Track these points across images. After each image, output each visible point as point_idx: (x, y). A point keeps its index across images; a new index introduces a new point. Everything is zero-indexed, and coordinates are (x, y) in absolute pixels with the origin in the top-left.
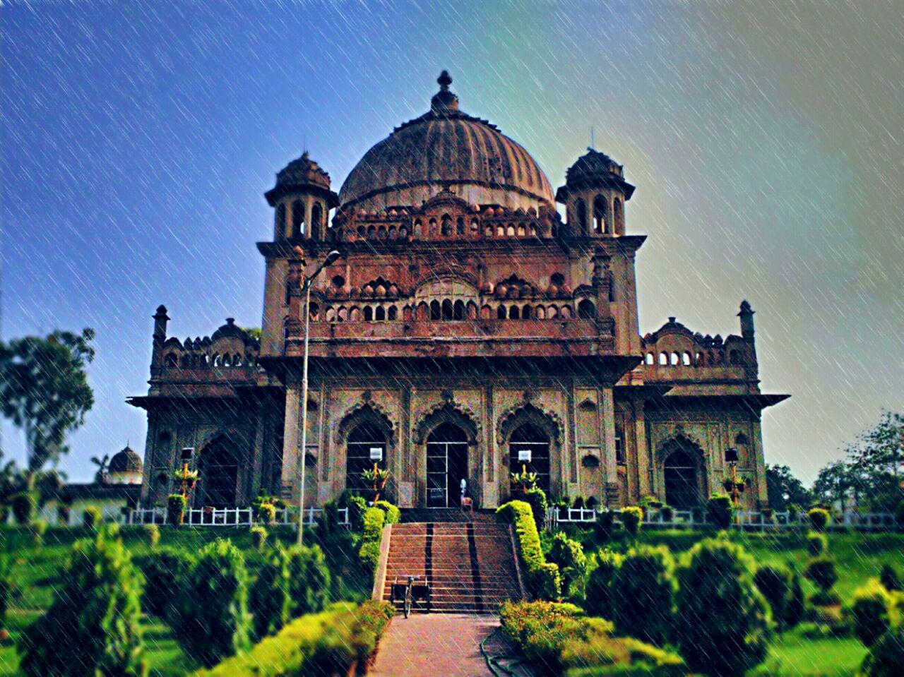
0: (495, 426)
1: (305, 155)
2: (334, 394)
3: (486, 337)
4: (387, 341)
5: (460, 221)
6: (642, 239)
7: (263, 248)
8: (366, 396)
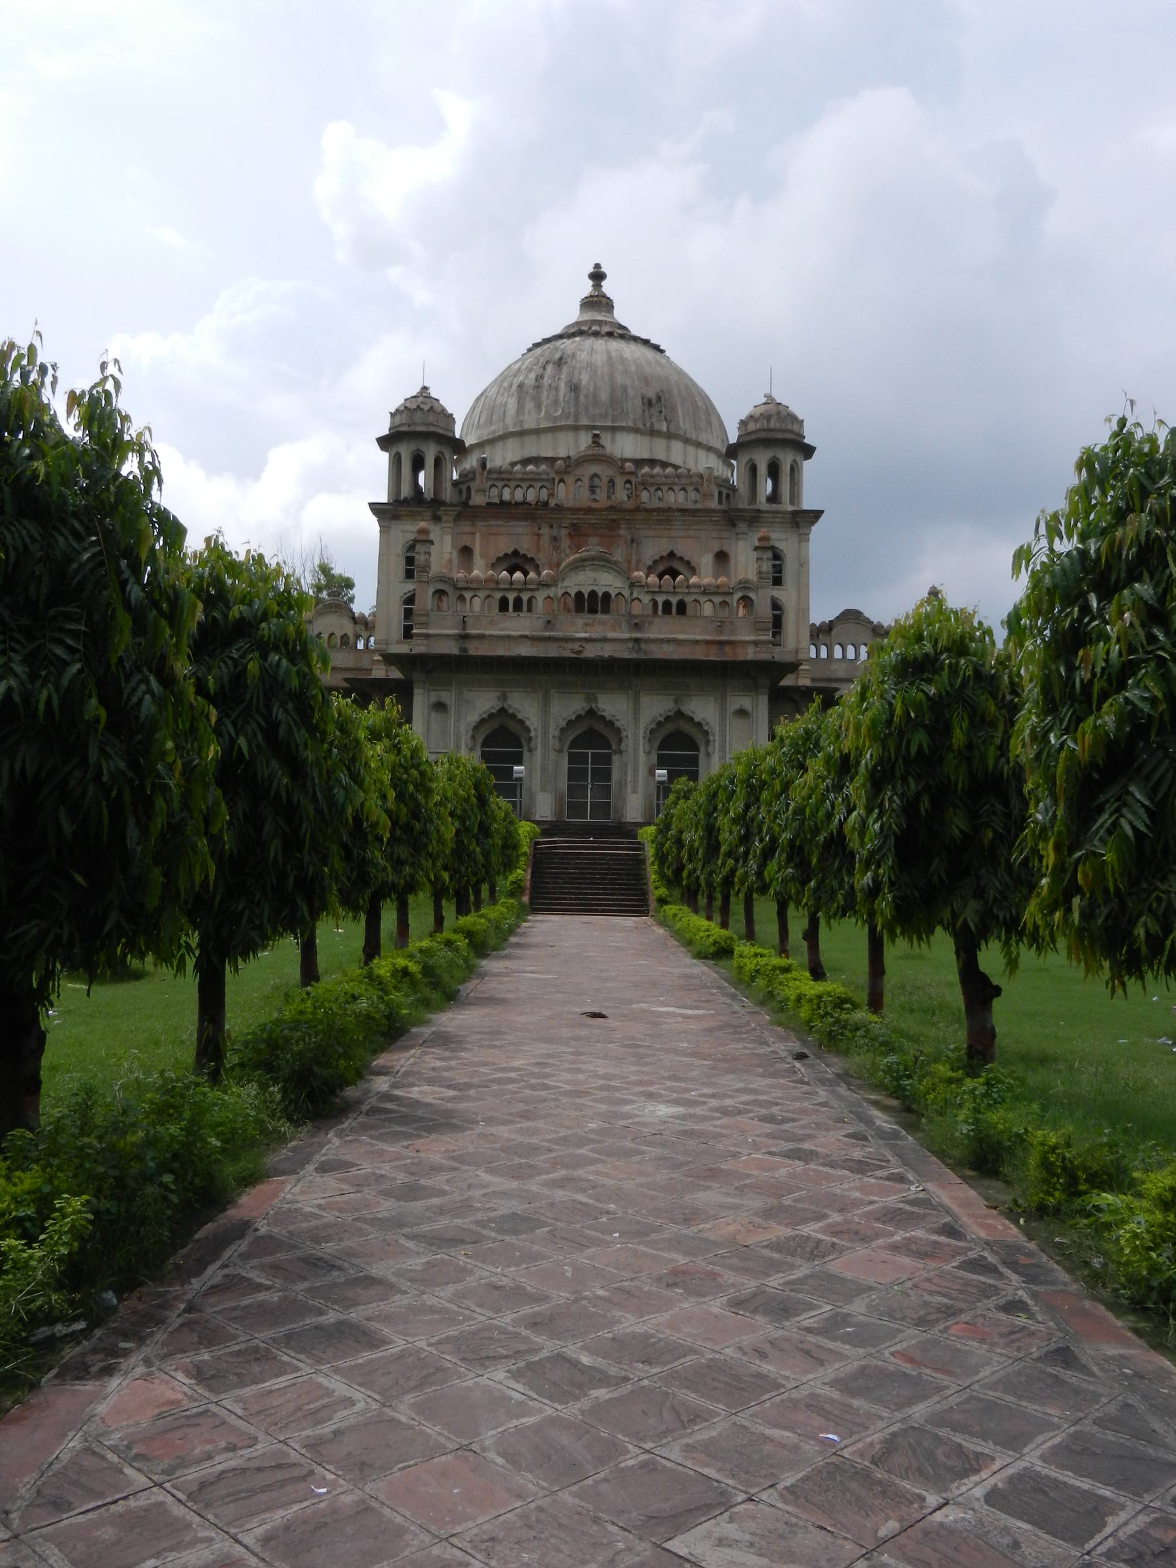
1: (425, 388)
2: (467, 695)
3: (635, 635)
4: (526, 637)
5: (612, 482)
6: (817, 514)
7: (376, 508)
8: (504, 697)
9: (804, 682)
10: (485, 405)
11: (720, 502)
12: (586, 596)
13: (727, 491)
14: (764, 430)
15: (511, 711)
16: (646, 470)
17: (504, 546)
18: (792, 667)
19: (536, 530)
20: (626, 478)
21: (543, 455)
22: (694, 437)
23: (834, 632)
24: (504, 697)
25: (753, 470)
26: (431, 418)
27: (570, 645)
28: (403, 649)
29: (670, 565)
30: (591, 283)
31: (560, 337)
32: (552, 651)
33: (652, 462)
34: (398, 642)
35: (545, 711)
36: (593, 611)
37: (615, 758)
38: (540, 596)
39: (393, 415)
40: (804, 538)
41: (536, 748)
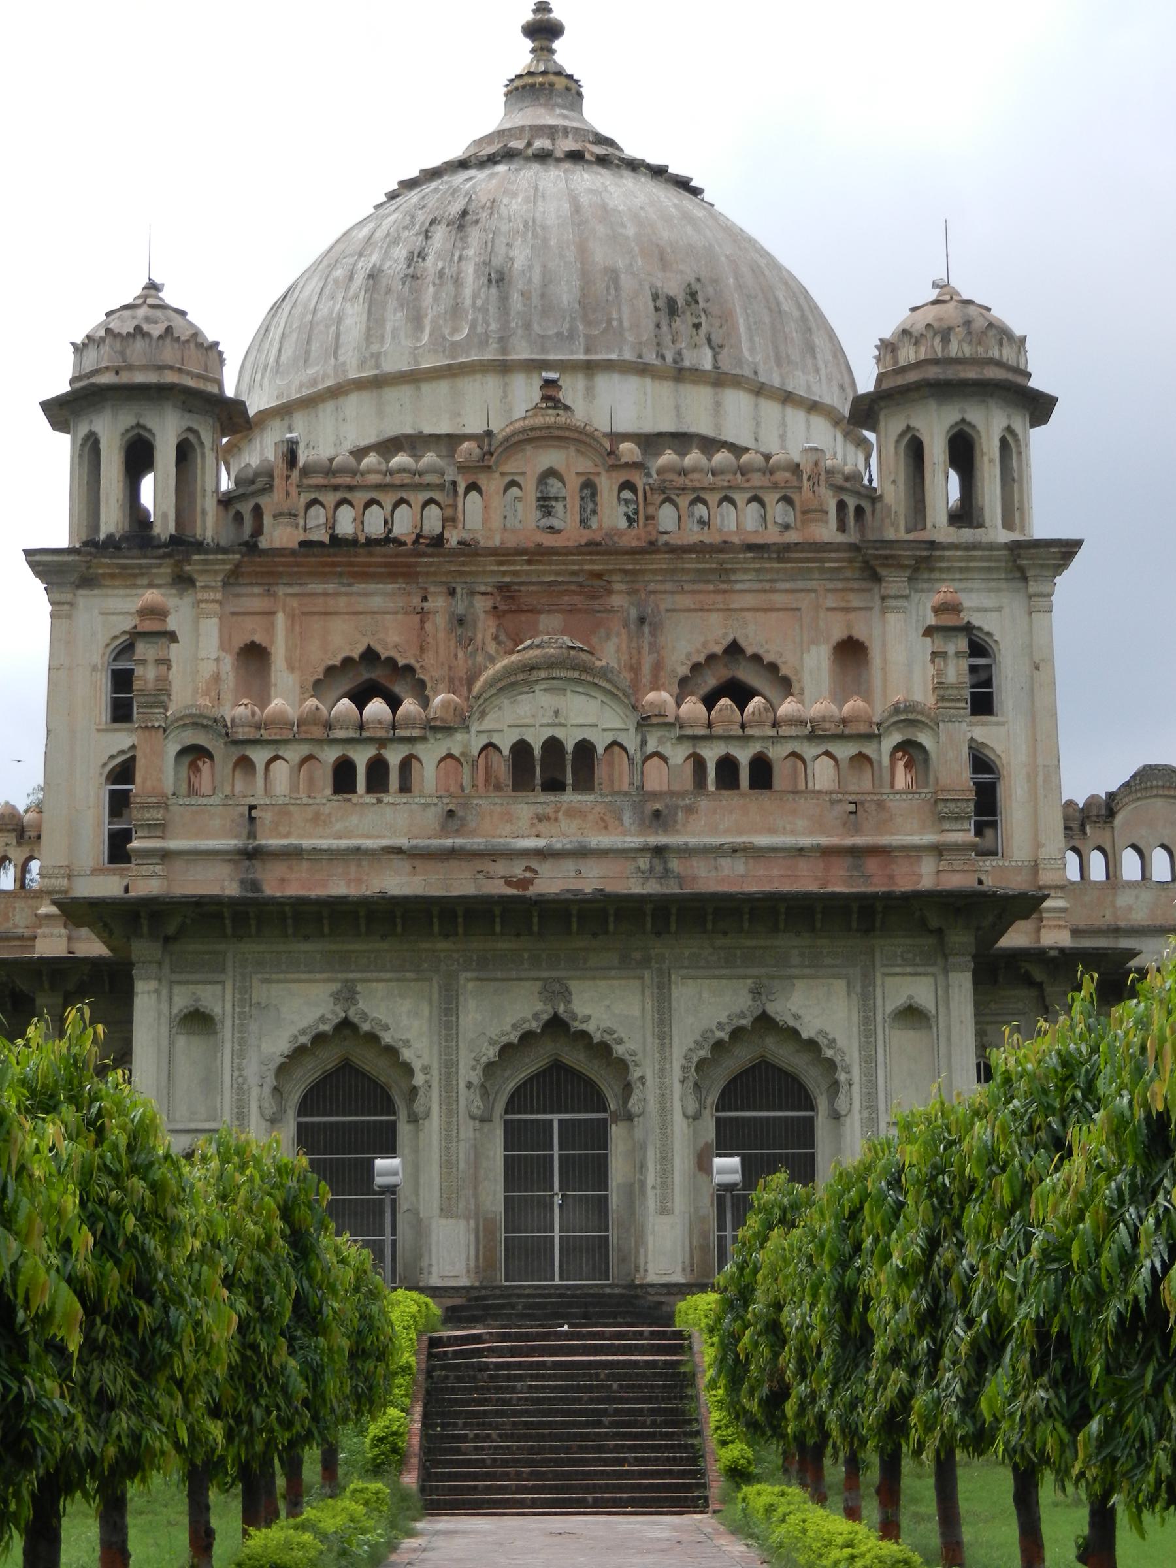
0: (677, 1074)
1: (153, 287)
2: (260, 992)
3: (654, 840)
4: (399, 851)
5: (589, 487)
6: (1067, 550)
7: (43, 563)
8: (348, 995)
9: (1055, 937)
10: (292, 320)
11: (842, 527)
12: (537, 751)
13: (857, 502)
14: (936, 362)
15: (366, 1027)
16: (668, 457)
17: (343, 640)
18: (1027, 904)
19: (416, 601)
20: (623, 476)
21: (428, 430)
22: (776, 383)
23: (1119, 820)
24: (348, 995)
25: (916, 451)
26: (169, 354)
27: (501, 868)
28: (109, 886)
29: (732, 679)
30: (528, 44)
31: (462, 164)
32: (461, 883)
33: (681, 440)
34: (96, 871)
35: (447, 1026)
36: (554, 785)
37: (616, 1132)
38: (430, 754)
39: (79, 349)
40: (1039, 603)
41: (428, 1115)
